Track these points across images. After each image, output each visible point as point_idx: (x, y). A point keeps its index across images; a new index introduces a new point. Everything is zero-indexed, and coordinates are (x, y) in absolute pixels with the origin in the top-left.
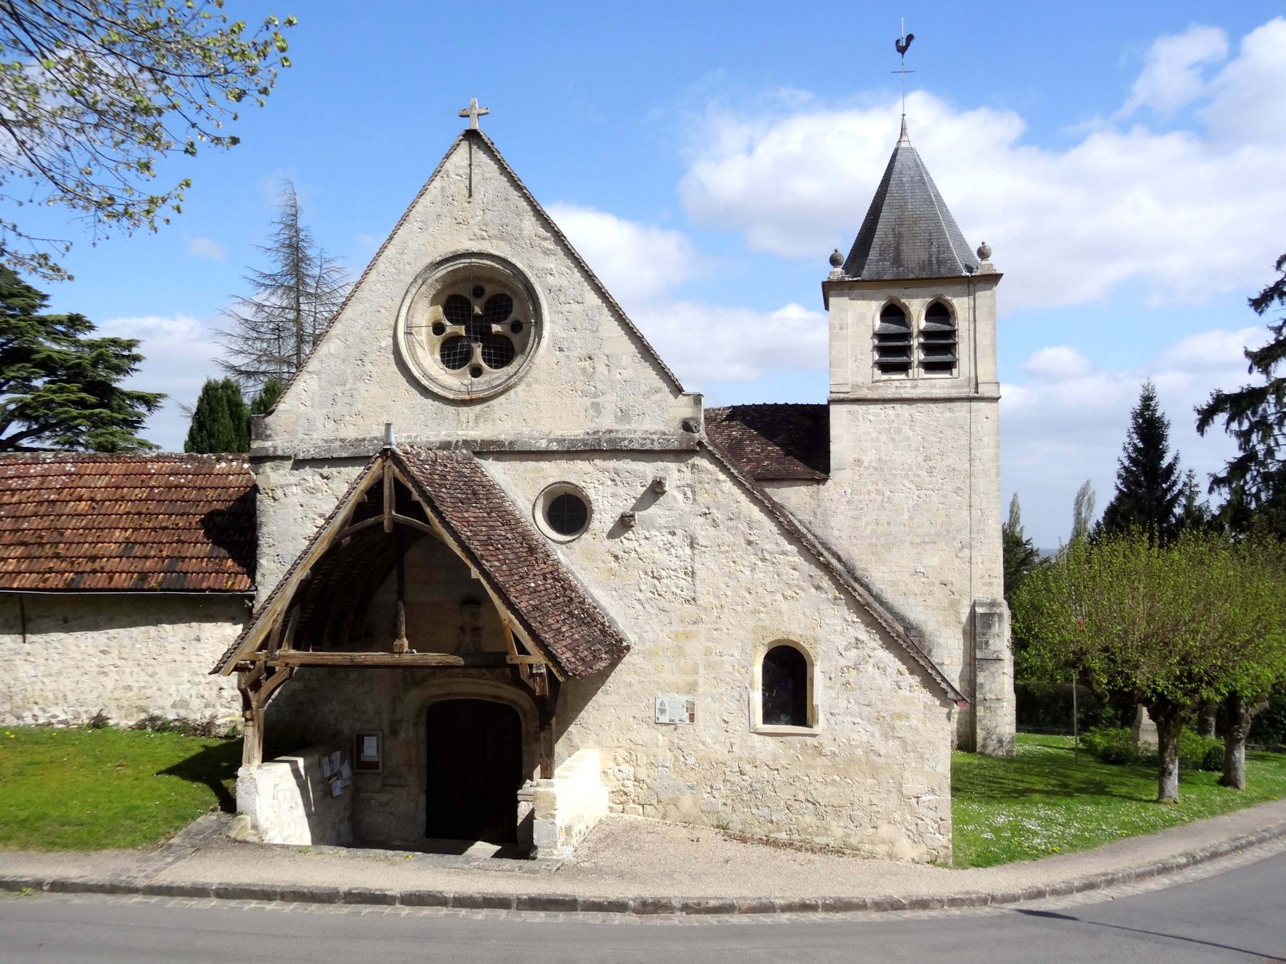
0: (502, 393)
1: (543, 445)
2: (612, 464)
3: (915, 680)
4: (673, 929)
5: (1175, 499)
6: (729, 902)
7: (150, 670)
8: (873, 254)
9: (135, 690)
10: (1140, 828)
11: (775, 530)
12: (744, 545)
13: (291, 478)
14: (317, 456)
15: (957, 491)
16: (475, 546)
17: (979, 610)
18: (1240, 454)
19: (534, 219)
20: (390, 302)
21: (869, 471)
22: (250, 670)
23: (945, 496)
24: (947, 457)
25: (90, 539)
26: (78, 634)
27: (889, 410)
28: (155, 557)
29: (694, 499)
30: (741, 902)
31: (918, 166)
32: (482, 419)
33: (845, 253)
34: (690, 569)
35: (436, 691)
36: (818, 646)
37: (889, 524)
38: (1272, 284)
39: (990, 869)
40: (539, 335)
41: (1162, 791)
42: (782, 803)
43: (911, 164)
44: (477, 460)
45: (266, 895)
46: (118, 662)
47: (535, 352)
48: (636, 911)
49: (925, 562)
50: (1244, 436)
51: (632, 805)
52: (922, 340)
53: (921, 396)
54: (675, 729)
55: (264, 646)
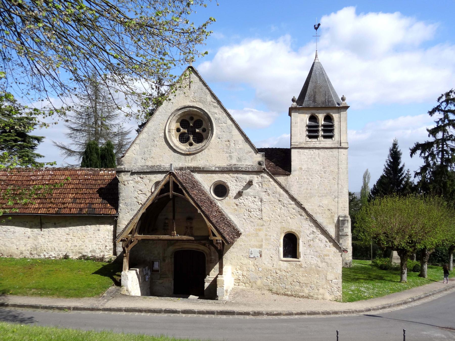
0: (200, 152)
1: (213, 169)
2: (236, 175)
3: (331, 244)
4: (265, 320)
5: (403, 179)
6: (280, 312)
7: (83, 240)
8: (306, 98)
9: (78, 246)
10: (396, 290)
11: (288, 197)
12: (278, 201)
13: (130, 178)
14: (139, 171)
15: (334, 179)
16: (199, 203)
17: (341, 219)
18: (425, 164)
19: (211, 96)
20: (163, 121)
21: (305, 172)
22: (126, 241)
23: (330, 180)
24: (331, 167)
25: (61, 197)
26: (59, 228)
27: (312, 151)
28: (84, 203)
29: (262, 187)
30: (283, 312)
31: (322, 68)
33: (297, 98)
35: (177, 247)
36: (301, 233)
37: (311, 189)
38: (436, 107)
39: (353, 303)
40: (212, 134)
41: (401, 279)
42: (289, 282)
43: (319, 68)
44: (192, 173)
45: (140, 311)
46: (72, 238)
47: (211, 139)
48: (252, 315)
49: (322, 202)
50: (426, 158)
51: (241, 283)
52: (322, 128)
53: (322, 147)
54: (255, 259)
55: (130, 233)
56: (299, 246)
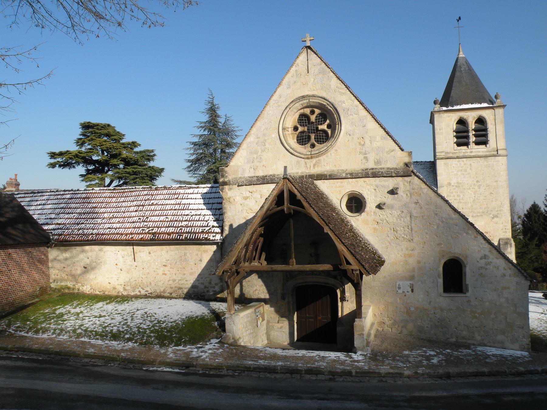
1: (344, 175)
23: (486, 197)
32: (316, 166)
34: (410, 227)
43: (465, 64)
52: (474, 133)
55: (235, 262)
56: (465, 275)
